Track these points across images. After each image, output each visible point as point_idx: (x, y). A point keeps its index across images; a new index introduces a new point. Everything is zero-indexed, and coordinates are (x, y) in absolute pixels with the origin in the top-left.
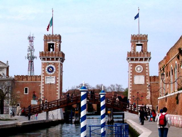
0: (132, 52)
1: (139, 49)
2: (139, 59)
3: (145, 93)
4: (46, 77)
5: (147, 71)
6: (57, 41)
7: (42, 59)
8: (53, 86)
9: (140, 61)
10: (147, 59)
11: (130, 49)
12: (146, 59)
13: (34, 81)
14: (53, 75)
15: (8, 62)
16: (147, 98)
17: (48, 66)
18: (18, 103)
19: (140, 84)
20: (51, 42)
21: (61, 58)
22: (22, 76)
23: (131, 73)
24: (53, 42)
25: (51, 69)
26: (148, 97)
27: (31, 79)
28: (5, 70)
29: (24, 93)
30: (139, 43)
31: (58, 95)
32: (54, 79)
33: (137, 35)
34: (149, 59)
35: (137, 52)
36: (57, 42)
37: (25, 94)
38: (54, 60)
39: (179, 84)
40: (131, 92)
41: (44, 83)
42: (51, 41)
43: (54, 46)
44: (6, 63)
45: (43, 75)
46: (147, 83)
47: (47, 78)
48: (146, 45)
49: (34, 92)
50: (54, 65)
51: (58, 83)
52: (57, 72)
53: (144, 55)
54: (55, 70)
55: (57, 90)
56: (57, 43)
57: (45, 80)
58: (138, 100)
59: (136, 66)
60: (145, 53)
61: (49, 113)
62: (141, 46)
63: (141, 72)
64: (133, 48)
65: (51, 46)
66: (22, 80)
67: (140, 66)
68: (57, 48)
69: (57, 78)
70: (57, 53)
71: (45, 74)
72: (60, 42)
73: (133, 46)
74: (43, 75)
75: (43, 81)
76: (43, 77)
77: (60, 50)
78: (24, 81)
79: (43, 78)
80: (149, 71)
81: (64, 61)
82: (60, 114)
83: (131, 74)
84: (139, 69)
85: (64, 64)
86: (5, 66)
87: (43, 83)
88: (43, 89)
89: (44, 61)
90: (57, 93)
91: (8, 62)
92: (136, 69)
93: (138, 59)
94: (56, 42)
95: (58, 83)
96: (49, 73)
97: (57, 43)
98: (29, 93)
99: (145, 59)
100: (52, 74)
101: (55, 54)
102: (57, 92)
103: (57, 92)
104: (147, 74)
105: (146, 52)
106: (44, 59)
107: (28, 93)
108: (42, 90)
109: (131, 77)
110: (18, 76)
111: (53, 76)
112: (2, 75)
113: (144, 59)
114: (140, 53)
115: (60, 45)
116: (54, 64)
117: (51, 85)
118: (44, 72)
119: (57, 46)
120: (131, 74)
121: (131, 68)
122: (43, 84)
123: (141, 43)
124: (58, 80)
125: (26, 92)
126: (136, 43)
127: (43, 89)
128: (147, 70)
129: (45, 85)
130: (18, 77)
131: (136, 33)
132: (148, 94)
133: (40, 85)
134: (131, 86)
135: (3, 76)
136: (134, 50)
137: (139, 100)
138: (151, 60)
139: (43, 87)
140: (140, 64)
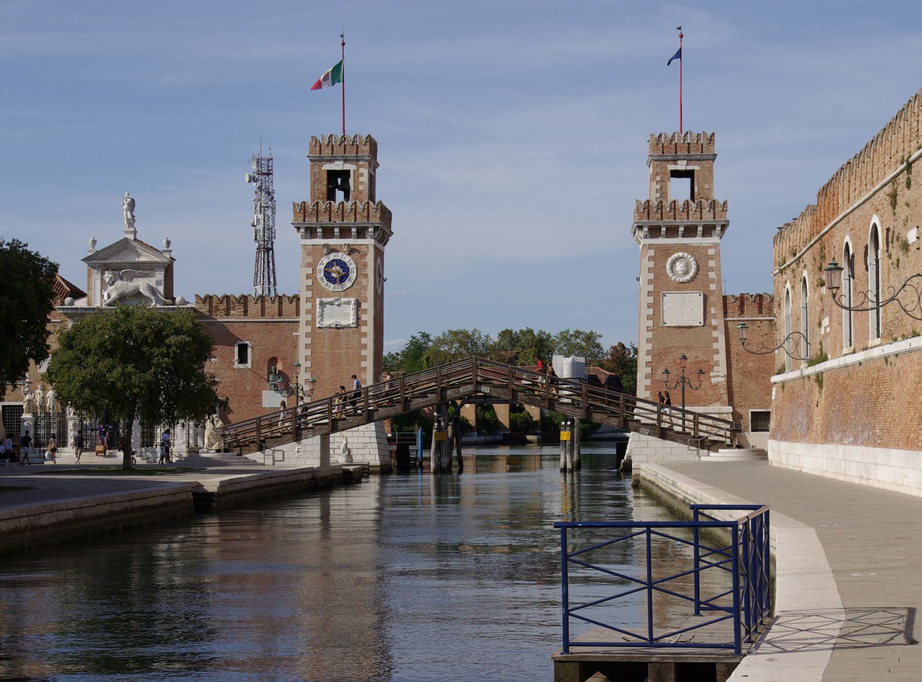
0: (654, 203)
1: (679, 190)
2: (681, 229)
3: (705, 359)
5: (712, 275)
6: (361, 163)
7: (302, 230)
9: (684, 236)
10: (714, 227)
11: (647, 192)
12: (708, 231)
14: (346, 293)
15: (168, 243)
16: (714, 380)
17: (325, 260)
20: (338, 166)
21: (376, 229)
22: (227, 297)
23: (650, 282)
24: (347, 167)
26: (718, 375)
27: (263, 309)
28: (160, 276)
29: (233, 363)
30: (681, 166)
31: (365, 372)
32: (351, 309)
33: (673, 136)
34: (718, 228)
35: (674, 201)
36: (361, 166)
37: (239, 369)
38: (350, 237)
39: (908, 308)
40: (649, 358)
41: (311, 323)
42: (336, 162)
43: (351, 181)
44: (162, 246)
45: (309, 294)
46: (714, 322)
47: (322, 304)
48: (707, 174)
50: (349, 254)
51: (365, 323)
52: (364, 282)
53: (701, 212)
54: (353, 275)
55: (364, 353)
56: (362, 170)
57: (318, 314)
58: (683, 389)
59: (670, 255)
60: (705, 203)
61: (331, 440)
62: (689, 180)
63: (688, 277)
64: (658, 187)
65: (339, 180)
66: (228, 314)
68: (361, 188)
69: (364, 306)
70: (360, 206)
71: (314, 288)
72: (373, 164)
73: (658, 178)
74: (309, 294)
75: (309, 317)
76: (308, 300)
77: (372, 197)
79: (309, 306)
80: (719, 276)
81: (387, 240)
82: (376, 445)
83: (651, 288)
84: (679, 267)
85: (388, 250)
87: (307, 323)
89: (311, 238)
90: (363, 364)
92: (668, 267)
93: (677, 227)
94: (359, 167)
95: (365, 323)
96: (332, 285)
97: (362, 170)
99: (704, 227)
101: (355, 211)
102: (365, 358)
103: (365, 358)
104: (713, 287)
105: (707, 199)
106: (311, 232)
107: (249, 365)
108: (303, 353)
109: (651, 300)
110: (211, 297)
111: (346, 296)
112: (146, 293)
113: (700, 229)
114: (687, 204)
115: (372, 179)
116: (352, 251)
118: (310, 282)
119: (361, 179)
120: (651, 288)
121: (652, 264)
122: (309, 329)
123: (690, 168)
124: (365, 311)
125: (243, 359)
126: (671, 167)
128: (712, 269)
129: (316, 333)
131: (669, 128)
132: (717, 364)
133: (296, 330)
134: (650, 335)
135: (153, 298)
136: (663, 192)
137: (687, 388)
138: (727, 231)
139: (309, 341)
140: (685, 248)
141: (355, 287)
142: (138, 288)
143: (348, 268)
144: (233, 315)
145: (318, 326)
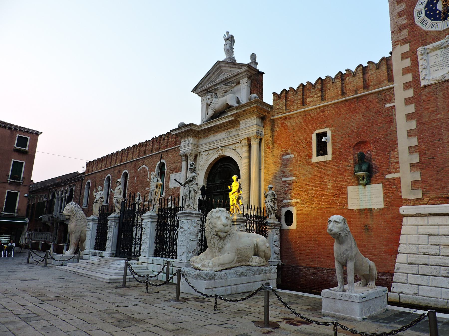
4: (420, 50)
13: (356, 92)
15: (253, 56)
18: (287, 205)
29: (311, 157)
37: (317, 163)
45: (406, 48)
49: (361, 144)
66: (304, 103)
74: (406, 48)
75: (409, 78)
76: (404, 56)
78: (314, 103)
79: (407, 63)
86: (240, 71)
87: (407, 86)
88: (409, 117)
91: (253, 56)
96: (440, 23)
98: (333, 154)
107: (329, 157)
108: (403, 126)
122: (410, 93)
130: (286, 97)
133: (391, 100)
142: (226, 101)
144: (310, 102)
145: (423, 83)
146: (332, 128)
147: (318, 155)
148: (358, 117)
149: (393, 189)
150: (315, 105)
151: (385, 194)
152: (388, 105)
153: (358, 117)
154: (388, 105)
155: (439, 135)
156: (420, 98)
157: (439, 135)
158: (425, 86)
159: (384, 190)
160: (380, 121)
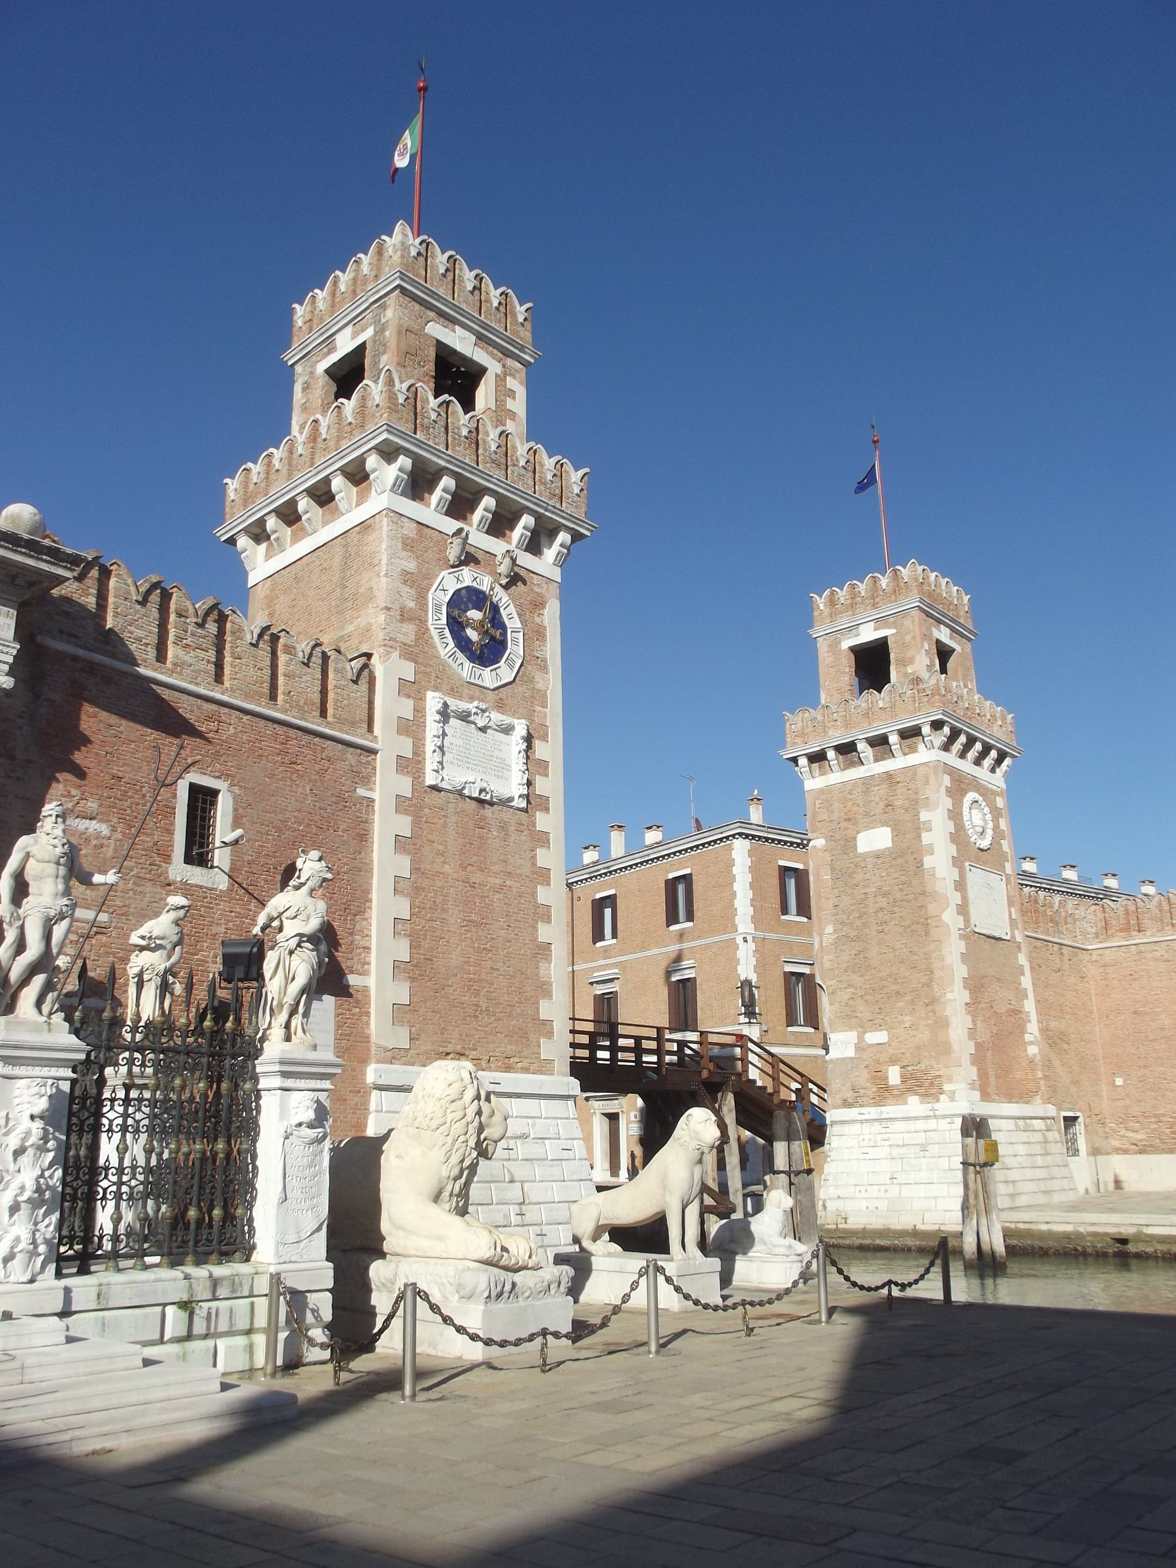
8: (504, 827)
19: (997, 935)
25: (474, 615)
29: (167, 858)
45: (408, 671)
67: (980, 799)
74: (408, 671)
75: (405, 747)
79: (406, 708)
100: (488, 677)
111: (500, 706)
117: (488, 811)
122: (405, 785)
127: (401, 844)
129: (424, 802)
139: (404, 825)
141: (519, 689)
143: (503, 627)
145: (430, 779)
146: (236, 790)
147: (189, 859)
148: (300, 790)
149: (354, 1015)
150: (197, 684)
151: (339, 1026)
152: (361, 792)
153: (300, 790)
154: (361, 792)
155: (444, 910)
156: (421, 808)
157: (444, 910)
158: (435, 788)
159: (337, 1015)
160: (344, 826)
